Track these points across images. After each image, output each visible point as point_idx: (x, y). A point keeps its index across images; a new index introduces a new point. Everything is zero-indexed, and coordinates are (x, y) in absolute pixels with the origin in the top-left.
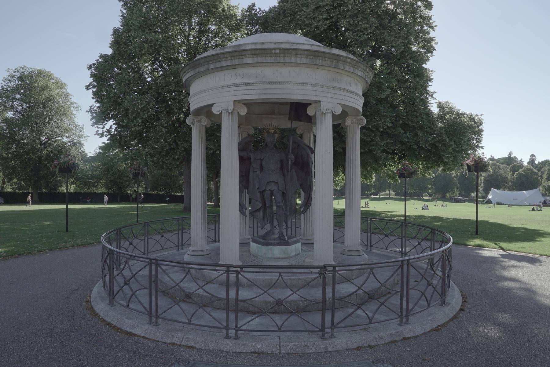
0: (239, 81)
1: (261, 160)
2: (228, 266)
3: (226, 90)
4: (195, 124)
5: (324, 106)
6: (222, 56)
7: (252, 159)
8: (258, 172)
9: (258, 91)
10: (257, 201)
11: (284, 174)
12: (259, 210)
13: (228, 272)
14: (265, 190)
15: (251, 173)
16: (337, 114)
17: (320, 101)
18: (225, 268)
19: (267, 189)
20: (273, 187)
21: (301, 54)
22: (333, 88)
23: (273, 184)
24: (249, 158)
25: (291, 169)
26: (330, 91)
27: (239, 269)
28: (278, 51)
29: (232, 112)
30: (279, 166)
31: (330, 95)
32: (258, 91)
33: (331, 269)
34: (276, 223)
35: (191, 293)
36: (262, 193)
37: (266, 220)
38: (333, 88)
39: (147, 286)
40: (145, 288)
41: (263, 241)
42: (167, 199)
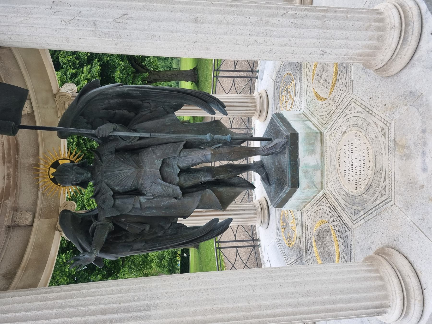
1: (116, 194)
8: (142, 199)
11: (146, 147)
24: (113, 219)
25: (135, 131)
36: (186, 191)
37: (236, 180)
41: (287, 189)
42: (185, 255)
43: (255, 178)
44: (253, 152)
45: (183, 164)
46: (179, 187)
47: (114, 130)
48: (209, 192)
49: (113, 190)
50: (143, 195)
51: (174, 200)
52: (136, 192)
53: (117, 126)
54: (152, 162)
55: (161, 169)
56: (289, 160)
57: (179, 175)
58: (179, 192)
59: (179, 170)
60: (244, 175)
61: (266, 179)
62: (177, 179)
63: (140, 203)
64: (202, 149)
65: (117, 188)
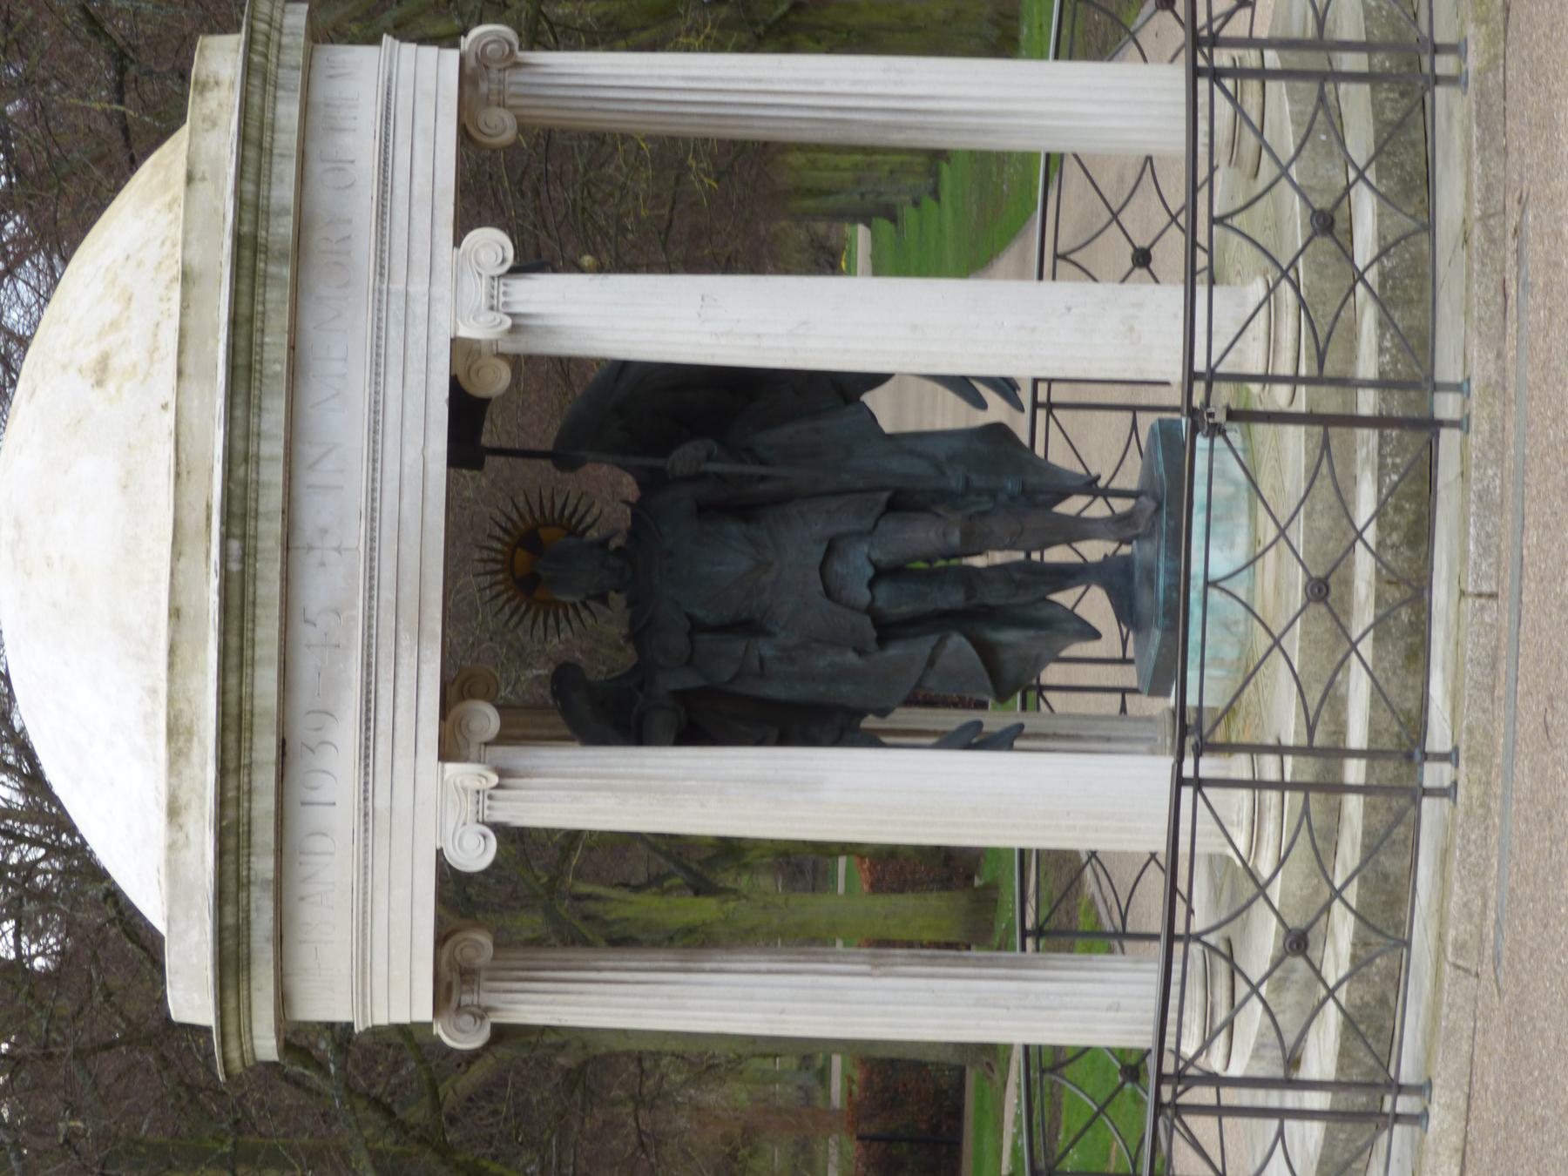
0: (346, 733)
1: (696, 627)
2: (1179, 781)
3: (382, 801)
4: (486, 999)
5: (481, 328)
6: (231, 812)
7: (691, 680)
8: (766, 649)
9: (407, 640)
10: (931, 662)
11: (783, 499)
12: (987, 652)
13: (1199, 784)
14: (871, 610)
15: (775, 690)
16: (510, 254)
17: (455, 342)
18: (1187, 793)
19: (864, 596)
20: (856, 565)
21: (247, 437)
22: (382, 270)
23: (838, 567)
26: (398, 286)
27: (1190, 741)
28: (235, 545)
29: (502, 773)
30: (734, 528)
31: (419, 288)
32: (407, 640)
33: (1199, 389)
34: (1057, 555)
35: (1289, 931)
36: (887, 630)
37: (1045, 612)
38: (382, 270)
39: (1273, 1124)
40: (1280, 1134)
43: (1094, 605)
44: (1075, 530)
45: (883, 556)
46: (868, 620)
47: (709, 458)
48: (957, 642)
49: (690, 617)
50: (769, 634)
51: (851, 658)
52: (749, 627)
53: (716, 449)
54: (798, 542)
55: (823, 568)
56: (1162, 558)
57: (872, 585)
58: (872, 634)
59: (870, 572)
60: (1065, 598)
61: (1127, 612)
62: (864, 596)
63: (762, 662)
64: (939, 516)
65: (700, 613)
